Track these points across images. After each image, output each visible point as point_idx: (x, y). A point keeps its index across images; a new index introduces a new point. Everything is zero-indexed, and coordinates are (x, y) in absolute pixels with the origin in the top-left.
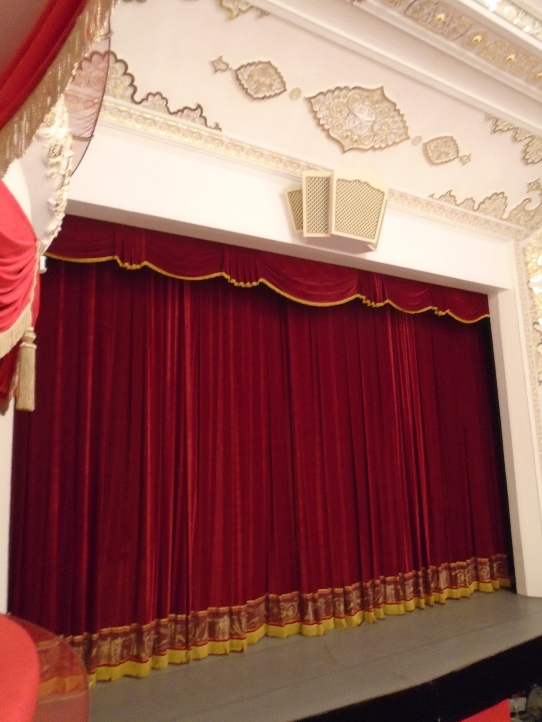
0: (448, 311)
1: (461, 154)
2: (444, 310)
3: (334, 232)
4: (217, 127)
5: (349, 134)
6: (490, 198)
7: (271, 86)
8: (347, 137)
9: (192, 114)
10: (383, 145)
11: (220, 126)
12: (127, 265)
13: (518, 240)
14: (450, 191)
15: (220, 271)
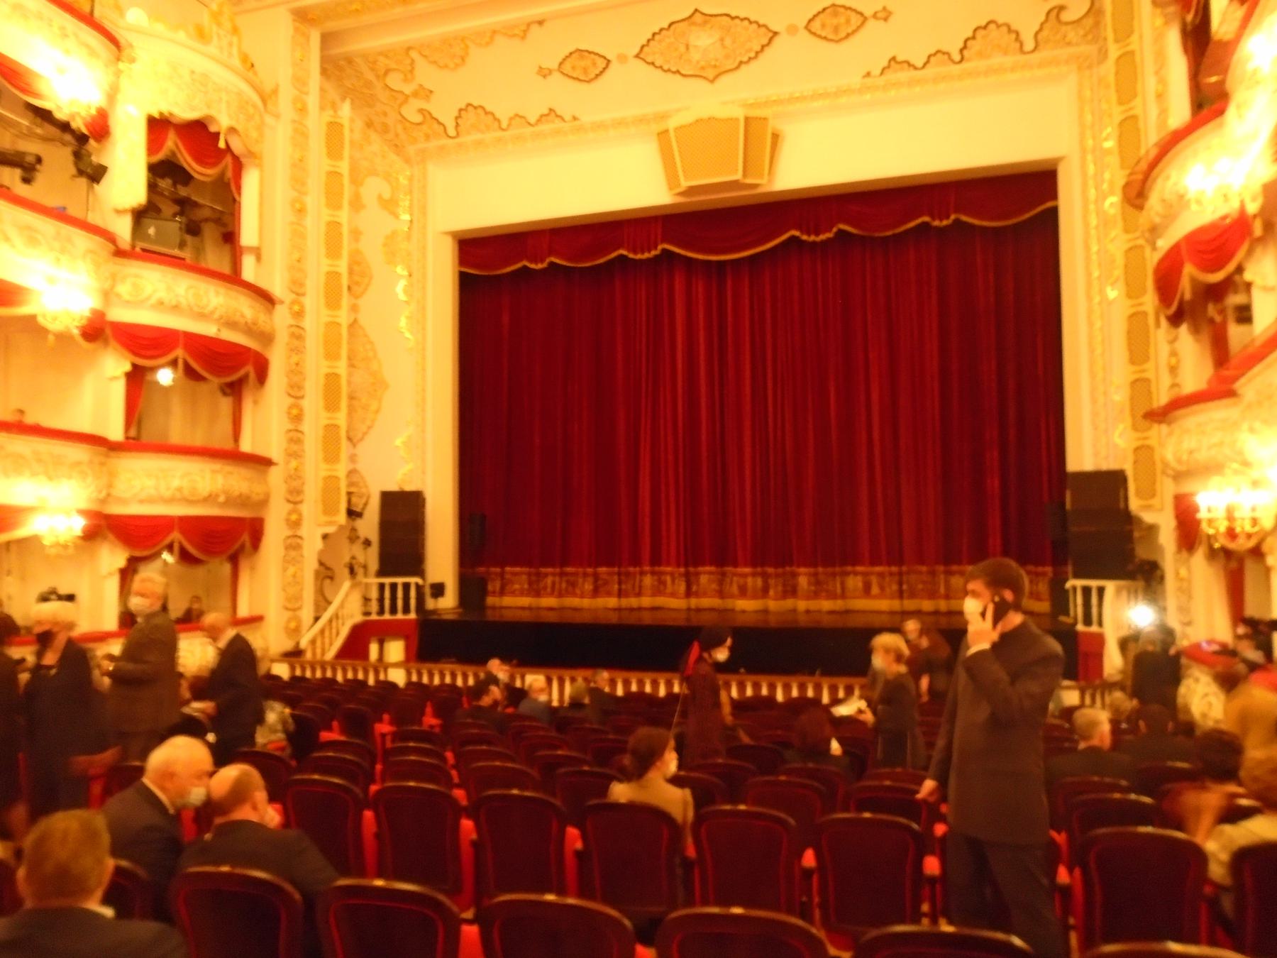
0: (953, 217)
1: (868, 13)
2: (948, 217)
3: (685, 184)
4: (575, 118)
5: (703, 63)
6: (974, 38)
7: (594, 64)
8: (703, 68)
9: (549, 118)
10: (752, 55)
11: (577, 115)
12: (533, 266)
13: (1090, 67)
14: (894, 59)
15: (618, 248)
